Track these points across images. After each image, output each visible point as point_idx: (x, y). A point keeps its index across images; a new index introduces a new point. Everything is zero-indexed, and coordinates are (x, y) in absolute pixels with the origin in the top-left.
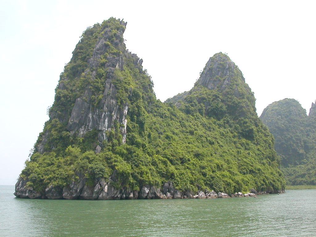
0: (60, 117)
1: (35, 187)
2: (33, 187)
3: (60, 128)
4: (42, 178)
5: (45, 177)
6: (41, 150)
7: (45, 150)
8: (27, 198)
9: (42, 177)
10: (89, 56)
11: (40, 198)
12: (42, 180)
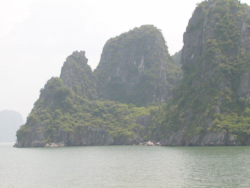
0: (228, 86)
1: (238, 138)
2: (237, 138)
3: (232, 94)
4: (244, 132)
5: (245, 131)
6: (218, 111)
7: (222, 112)
8: (234, 145)
9: (243, 130)
10: (239, 37)
11: (240, 145)
12: (243, 133)
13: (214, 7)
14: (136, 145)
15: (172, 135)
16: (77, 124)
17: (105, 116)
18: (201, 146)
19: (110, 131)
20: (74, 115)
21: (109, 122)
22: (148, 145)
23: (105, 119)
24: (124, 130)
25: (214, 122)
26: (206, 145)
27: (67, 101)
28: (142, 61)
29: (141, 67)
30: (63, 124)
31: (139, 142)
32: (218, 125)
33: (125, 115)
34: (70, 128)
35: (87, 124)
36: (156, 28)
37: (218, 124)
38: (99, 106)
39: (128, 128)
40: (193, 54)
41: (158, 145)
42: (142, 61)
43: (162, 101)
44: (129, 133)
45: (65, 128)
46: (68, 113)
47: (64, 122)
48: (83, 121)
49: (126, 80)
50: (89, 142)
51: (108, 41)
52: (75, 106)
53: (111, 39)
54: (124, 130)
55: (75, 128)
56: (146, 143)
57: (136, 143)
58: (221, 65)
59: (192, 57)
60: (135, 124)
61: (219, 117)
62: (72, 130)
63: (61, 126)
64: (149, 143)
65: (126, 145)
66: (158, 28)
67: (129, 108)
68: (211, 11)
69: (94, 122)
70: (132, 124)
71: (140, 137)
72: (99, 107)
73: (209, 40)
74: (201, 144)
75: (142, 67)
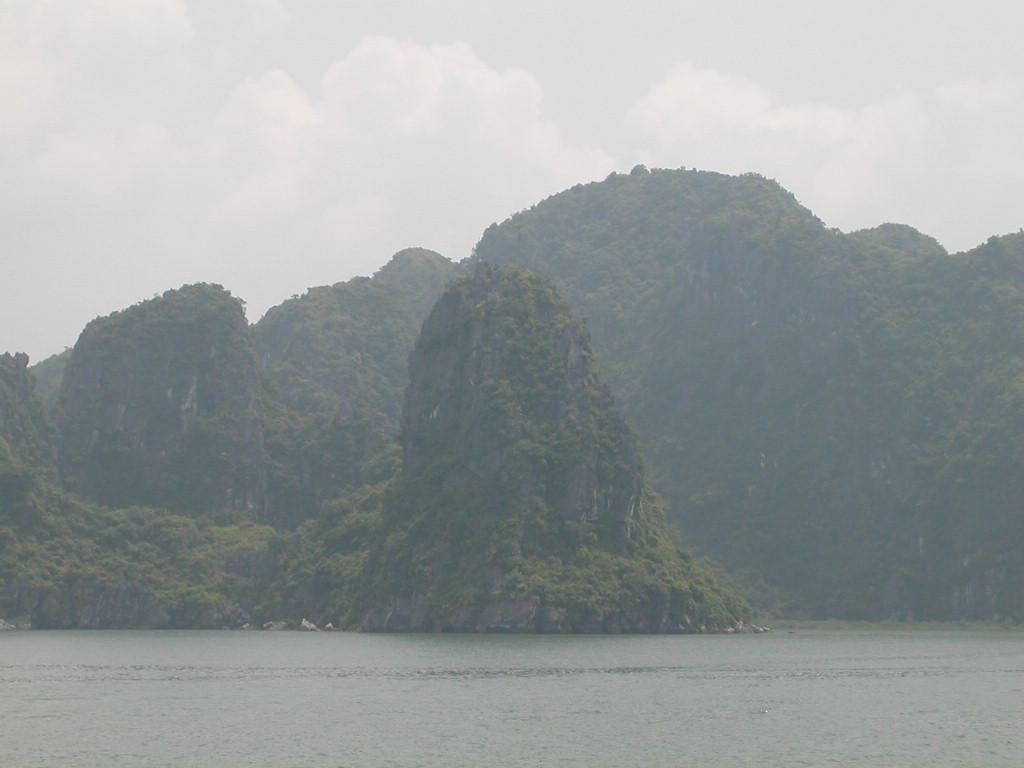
13: (499, 300)
14: (232, 628)
15: (390, 605)
16: (62, 570)
17: (134, 548)
18: (476, 632)
19: (156, 589)
20: (48, 542)
21: (152, 565)
22: (306, 629)
23: (135, 556)
24: (193, 588)
25: (508, 577)
26: (489, 631)
27: (30, 504)
28: (192, 391)
29: (187, 405)
30: (23, 566)
31: (239, 621)
32: (521, 585)
33: (191, 547)
34: (46, 578)
35: (91, 569)
36: (229, 293)
37: (520, 582)
38: (116, 518)
39: (204, 584)
40: (437, 409)
41: (329, 629)
42: (192, 391)
43: (251, 506)
44: (213, 597)
45: (31, 578)
46: (33, 538)
47: (28, 563)
48: (77, 561)
49: (142, 444)
50: (98, 620)
51: (89, 325)
52: (51, 519)
53: (99, 321)
54: (193, 588)
55: (58, 580)
56: (271, 625)
57: (231, 623)
58: (524, 443)
59: (435, 413)
60: (224, 574)
61: (520, 566)
62: (49, 584)
63: (19, 574)
64: (305, 622)
65: (202, 627)
66: (234, 295)
67: (200, 528)
68: (492, 309)
69: (107, 564)
70: (214, 573)
71: (240, 610)
72: (115, 524)
73: (491, 382)
74: (478, 628)
75: (192, 407)
